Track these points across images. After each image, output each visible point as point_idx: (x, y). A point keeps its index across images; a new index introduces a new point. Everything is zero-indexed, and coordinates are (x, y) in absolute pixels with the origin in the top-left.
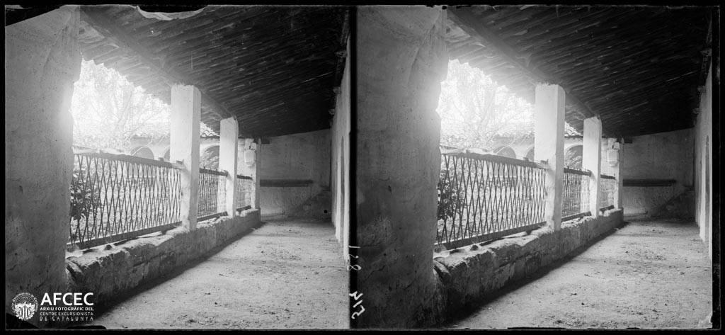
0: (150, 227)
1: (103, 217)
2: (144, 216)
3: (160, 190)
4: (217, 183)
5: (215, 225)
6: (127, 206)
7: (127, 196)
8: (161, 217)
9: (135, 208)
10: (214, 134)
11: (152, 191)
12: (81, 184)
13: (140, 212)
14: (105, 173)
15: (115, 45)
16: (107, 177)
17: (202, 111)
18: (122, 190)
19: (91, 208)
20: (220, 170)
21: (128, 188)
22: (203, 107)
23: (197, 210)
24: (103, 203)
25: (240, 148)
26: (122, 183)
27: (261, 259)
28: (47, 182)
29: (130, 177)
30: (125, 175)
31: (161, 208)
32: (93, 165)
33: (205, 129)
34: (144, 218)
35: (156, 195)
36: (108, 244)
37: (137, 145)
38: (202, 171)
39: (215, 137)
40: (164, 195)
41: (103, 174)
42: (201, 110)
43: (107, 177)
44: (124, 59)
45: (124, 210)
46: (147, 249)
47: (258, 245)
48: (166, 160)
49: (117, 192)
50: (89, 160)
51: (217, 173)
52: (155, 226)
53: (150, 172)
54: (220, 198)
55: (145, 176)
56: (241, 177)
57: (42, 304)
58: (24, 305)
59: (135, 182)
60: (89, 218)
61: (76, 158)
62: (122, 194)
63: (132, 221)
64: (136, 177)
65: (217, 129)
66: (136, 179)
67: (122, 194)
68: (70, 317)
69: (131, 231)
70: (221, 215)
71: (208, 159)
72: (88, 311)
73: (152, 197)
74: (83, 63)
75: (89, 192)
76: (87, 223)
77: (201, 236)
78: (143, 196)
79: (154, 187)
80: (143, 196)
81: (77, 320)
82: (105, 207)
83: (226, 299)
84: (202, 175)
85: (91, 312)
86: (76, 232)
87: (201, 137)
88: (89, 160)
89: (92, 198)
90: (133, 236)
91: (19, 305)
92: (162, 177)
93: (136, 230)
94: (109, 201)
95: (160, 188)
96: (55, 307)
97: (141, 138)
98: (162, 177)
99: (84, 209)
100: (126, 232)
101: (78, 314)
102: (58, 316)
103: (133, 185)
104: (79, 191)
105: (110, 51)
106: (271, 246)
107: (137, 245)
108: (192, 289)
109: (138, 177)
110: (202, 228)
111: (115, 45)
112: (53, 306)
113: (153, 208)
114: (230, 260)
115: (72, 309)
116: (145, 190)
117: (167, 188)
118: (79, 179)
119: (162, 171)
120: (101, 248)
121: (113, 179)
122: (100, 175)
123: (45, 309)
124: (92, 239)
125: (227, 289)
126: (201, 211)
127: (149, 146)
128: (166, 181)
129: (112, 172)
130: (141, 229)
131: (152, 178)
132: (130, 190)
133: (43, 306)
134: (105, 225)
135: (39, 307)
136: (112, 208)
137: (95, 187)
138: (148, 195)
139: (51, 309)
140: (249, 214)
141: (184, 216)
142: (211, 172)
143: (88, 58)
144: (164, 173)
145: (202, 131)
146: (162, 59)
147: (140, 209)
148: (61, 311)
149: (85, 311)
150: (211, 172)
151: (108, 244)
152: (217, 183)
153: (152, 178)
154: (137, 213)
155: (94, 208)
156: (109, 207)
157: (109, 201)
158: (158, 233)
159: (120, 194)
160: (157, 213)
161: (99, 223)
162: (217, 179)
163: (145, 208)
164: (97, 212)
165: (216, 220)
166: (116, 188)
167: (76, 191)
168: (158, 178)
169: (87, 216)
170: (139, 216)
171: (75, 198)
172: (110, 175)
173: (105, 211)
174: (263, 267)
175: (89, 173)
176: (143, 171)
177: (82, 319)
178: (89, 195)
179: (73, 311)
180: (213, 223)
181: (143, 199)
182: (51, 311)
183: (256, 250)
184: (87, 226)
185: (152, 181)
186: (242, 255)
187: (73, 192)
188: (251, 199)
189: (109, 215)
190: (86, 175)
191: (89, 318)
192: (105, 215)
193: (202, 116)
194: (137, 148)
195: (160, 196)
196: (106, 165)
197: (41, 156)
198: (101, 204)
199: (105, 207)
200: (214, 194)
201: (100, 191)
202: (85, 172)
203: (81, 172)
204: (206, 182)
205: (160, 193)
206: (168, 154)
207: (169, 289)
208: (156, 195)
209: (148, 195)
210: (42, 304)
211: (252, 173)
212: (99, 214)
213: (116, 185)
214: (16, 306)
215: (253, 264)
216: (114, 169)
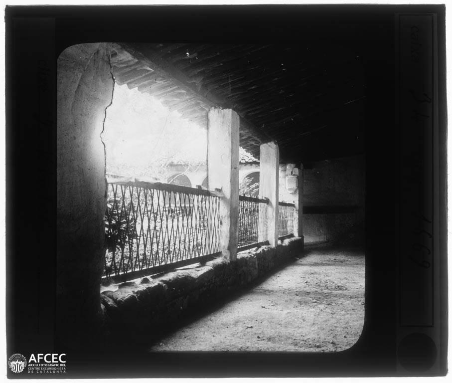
0: (189, 258)
1: (140, 247)
2: (182, 247)
3: (198, 219)
4: (258, 210)
5: (256, 254)
6: (164, 236)
7: (164, 226)
8: (199, 247)
9: (172, 238)
10: (254, 159)
11: (190, 220)
12: (115, 215)
13: (177, 243)
14: (141, 202)
15: (149, 69)
16: (143, 206)
17: (241, 135)
18: (158, 220)
19: (127, 240)
20: (260, 197)
21: (164, 218)
22: (242, 132)
23: (237, 240)
24: (139, 234)
25: (281, 174)
26: (159, 213)
27: (305, 289)
28: (80, 213)
29: (167, 206)
30: (162, 204)
31: (199, 238)
32: (127, 195)
33: (244, 155)
34: (182, 249)
35: (194, 225)
36: (145, 277)
37: (174, 173)
38: (243, 198)
39: (255, 163)
40: (202, 224)
41: (139, 204)
42: (240, 133)
43: (143, 206)
44: (160, 83)
45: (161, 241)
46: (187, 280)
47: (303, 275)
48: (204, 188)
49: (153, 222)
50: (123, 189)
51: (257, 201)
52: (193, 257)
53: (187, 200)
54: (261, 228)
55: (183, 205)
56: (283, 204)
57: (30, 362)
58: (17, 362)
59: (172, 211)
60: (125, 250)
61: (110, 187)
62: (158, 225)
63: (169, 252)
64: (173, 206)
65: (257, 154)
66: (173, 208)
67: (158, 225)
68: (49, 370)
69: (169, 262)
70: (262, 244)
71: (248, 186)
72: (62, 367)
73: (190, 227)
74: (117, 87)
75: (124, 223)
76: (122, 256)
77: (242, 267)
78: (180, 226)
79: (192, 216)
80: (180, 226)
81: (54, 372)
82: (142, 238)
83: (270, 332)
84: (241, 203)
85: (64, 367)
86: (111, 265)
87: (241, 163)
88: (123, 189)
89: (127, 228)
90: (171, 268)
91: (14, 362)
92: (200, 206)
93: (174, 261)
94: (145, 232)
95: (198, 217)
96: (39, 363)
97: (177, 165)
98: (200, 206)
99: (119, 240)
100: (163, 264)
101: (55, 369)
102: (40, 370)
103: (170, 214)
104: (114, 222)
105: (144, 75)
106: (315, 275)
107: (175, 277)
108: (232, 323)
109: (176, 206)
110: (243, 259)
111: (149, 69)
112: (37, 363)
113: (192, 238)
114: (273, 291)
115: (51, 365)
116: (183, 220)
117: (206, 217)
118: (113, 209)
119: (200, 200)
120: (138, 281)
121: (149, 208)
122: (135, 204)
123: (31, 365)
124: (128, 272)
125: (271, 322)
126: (241, 240)
127: (186, 173)
128: (204, 210)
129: (148, 202)
130: (179, 260)
131: (190, 207)
132: (167, 219)
133: (30, 363)
134: (141, 257)
135: (28, 363)
136: (149, 239)
137: (131, 217)
138: (185, 225)
139: (36, 365)
140: (291, 243)
141: (224, 246)
142: (250, 200)
143: (122, 82)
144: (202, 202)
145: (241, 156)
146: (198, 82)
147: (178, 240)
148: (43, 367)
149: (60, 367)
150: (250, 200)
151: (145, 277)
152: (258, 212)
153: (190, 207)
154: (175, 244)
155: (129, 239)
156: (145, 238)
157: (145, 232)
158: (197, 264)
159: (157, 224)
160: (195, 243)
161: (135, 255)
162: (258, 207)
163: (182, 239)
164: (133, 243)
165: (257, 250)
166: (152, 218)
167: (110, 222)
168: (196, 207)
169: (123, 248)
170: (177, 246)
171: (109, 230)
172: (146, 203)
173: (142, 242)
174: (308, 298)
175: (124, 203)
176: (180, 199)
177: (58, 372)
178: (124, 225)
179: (51, 367)
180: (255, 253)
181: (180, 229)
182: (36, 367)
183: (300, 280)
184: (122, 258)
185: (190, 210)
186: (285, 286)
187: (107, 223)
188: (293, 226)
189: (145, 246)
190: (121, 205)
191: (63, 372)
192: (142, 247)
193: (240, 141)
194: (174, 176)
195: (198, 225)
196: (141, 194)
197: (74, 186)
198: (137, 236)
199: (142, 238)
200: (254, 223)
201: (135, 222)
202: (119, 202)
203: (115, 202)
204: (246, 210)
205: (198, 222)
206: (207, 181)
207: (209, 322)
208: (194, 225)
209: (185, 225)
210: (30, 362)
211: (294, 199)
212: (135, 245)
213: (152, 215)
214: (11, 363)
215: (297, 295)
216: (150, 198)
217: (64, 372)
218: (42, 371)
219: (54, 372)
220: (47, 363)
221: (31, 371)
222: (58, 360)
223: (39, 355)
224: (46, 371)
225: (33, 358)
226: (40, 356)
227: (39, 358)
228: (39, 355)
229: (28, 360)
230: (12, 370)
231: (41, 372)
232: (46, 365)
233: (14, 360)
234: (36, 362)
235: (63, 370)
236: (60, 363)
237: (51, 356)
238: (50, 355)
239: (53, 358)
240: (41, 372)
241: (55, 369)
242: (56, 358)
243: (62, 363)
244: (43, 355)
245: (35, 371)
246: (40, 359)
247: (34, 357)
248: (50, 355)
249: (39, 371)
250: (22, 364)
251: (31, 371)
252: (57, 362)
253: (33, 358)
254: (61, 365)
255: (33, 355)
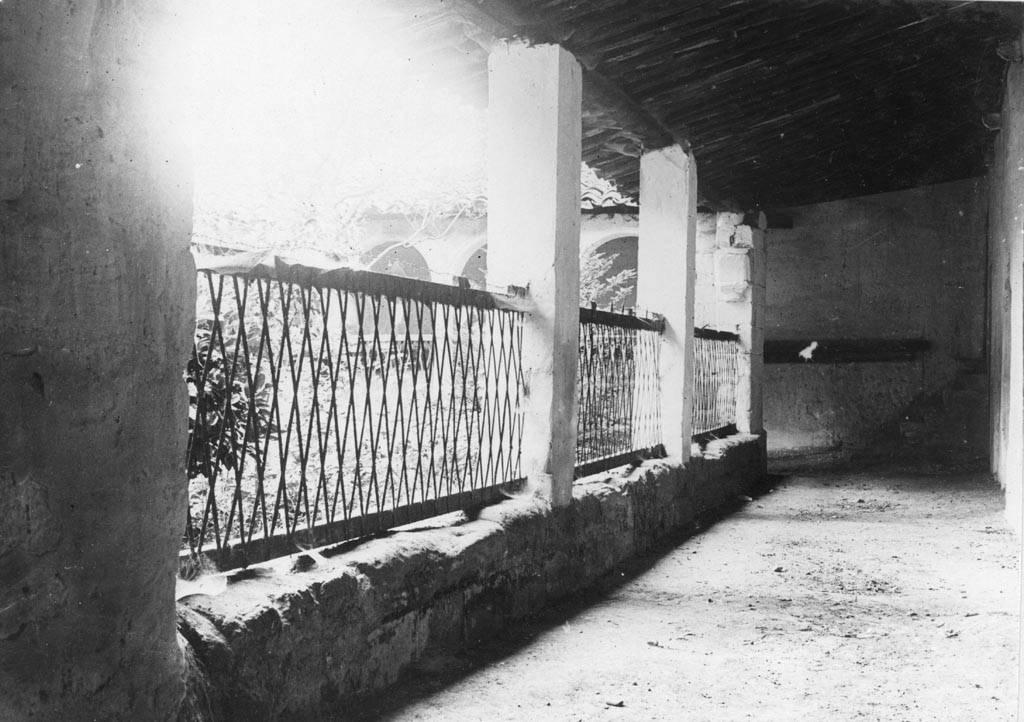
5: (628, 486)
10: (620, 199)
20: (640, 314)
22: (587, 114)
25: (701, 243)
27: (775, 592)
36: (305, 552)
37: (377, 239)
38: (589, 317)
39: (620, 209)
46: (425, 564)
47: (767, 548)
51: (631, 323)
61: (202, 281)
70: (646, 454)
71: (602, 280)
110: (590, 499)
120: (282, 565)
127: (415, 240)
140: (731, 451)
142: (609, 320)
150: (609, 320)
158: (457, 515)
174: (785, 618)
176: (407, 319)
180: (624, 481)
183: (760, 563)
186: (717, 582)
188: (736, 404)
194: (380, 248)
211: (739, 318)
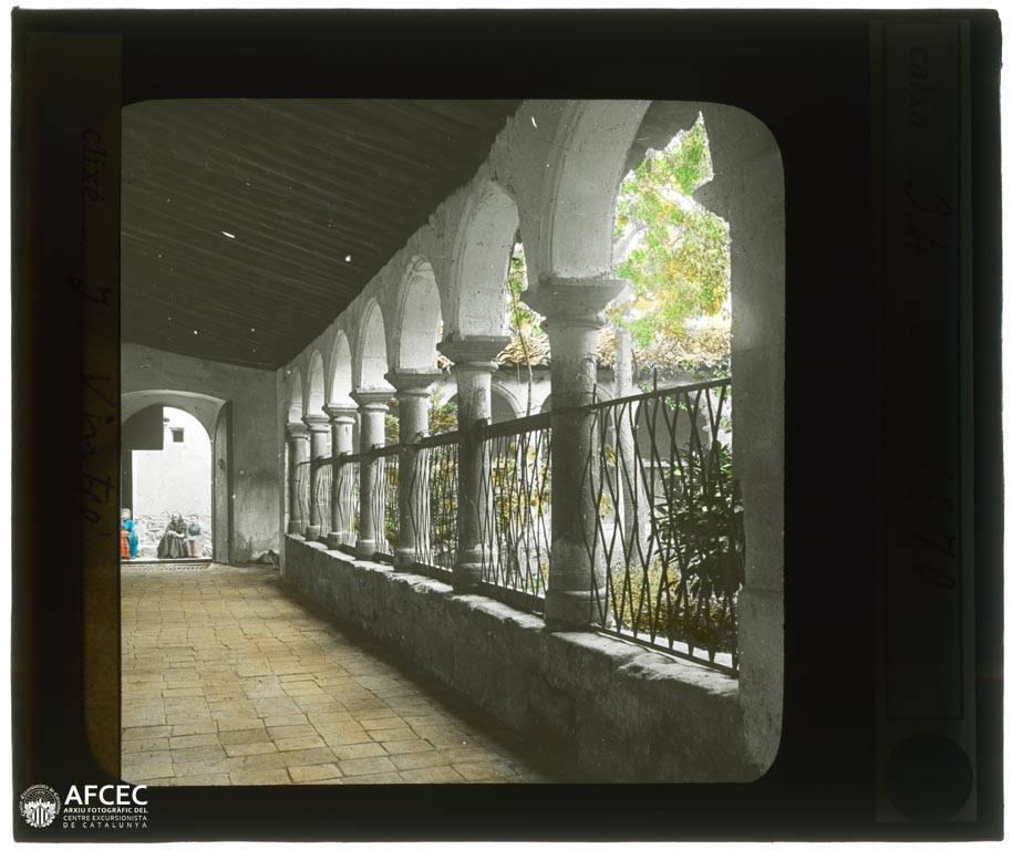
57: (67, 802)
58: (38, 804)
68: (110, 822)
85: (143, 814)
91: (31, 804)
96: (86, 807)
101: (123, 818)
112: (84, 806)
115: (114, 810)
123: (71, 810)
133: (68, 806)
135: (63, 806)
148: (97, 814)
149: (133, 814)
179: (114, 814)
182: (81, 814)
210: (67, 802)
217: (144, 825)
218: (95, 823)
219: (121, 827)
220: (107, 806)
221: (69, 823)
222: (129, 798)
223: (87, 788)
224: (104, 823)
225: (74, 795)
226: (91, 791)
227: (87, 795)
228: (87, 788)
229: (63, 800)
230: (28, 821)
231: (92, 825)
232: (104, 810)
233: (33, 798)
234: (80, 803)
235: (141, 822)
236: (133, 805)
237: (115, 791)
238: (112, 787)
239: (119, 795)
240: (92, 825)
241: (123, 818)
242: (126, 795)
243: (139, 806)
244: (96, 787)
245: (78, 823)
246: (90, 797)
247: (77, 794)
248: (112, 787)
249: (88, 824)
250: (51, 808)
251: (69, 823)
252: (128, 803)
253: (74, 795)
254: (136, 810)
255: (74, 788)
